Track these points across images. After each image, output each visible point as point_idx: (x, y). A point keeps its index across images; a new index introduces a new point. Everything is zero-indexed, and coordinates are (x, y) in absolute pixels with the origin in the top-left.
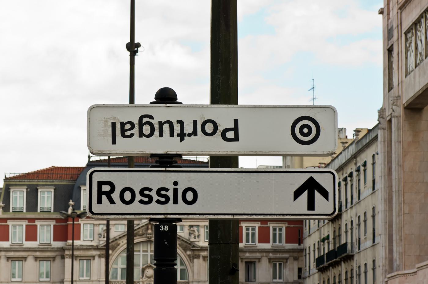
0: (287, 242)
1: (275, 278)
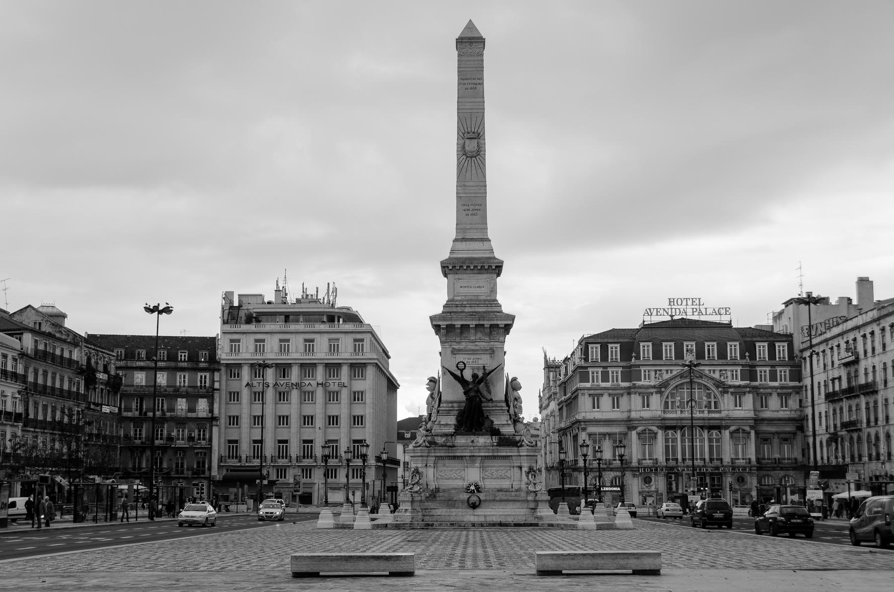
0: (790, 381)
1: (782, 407)
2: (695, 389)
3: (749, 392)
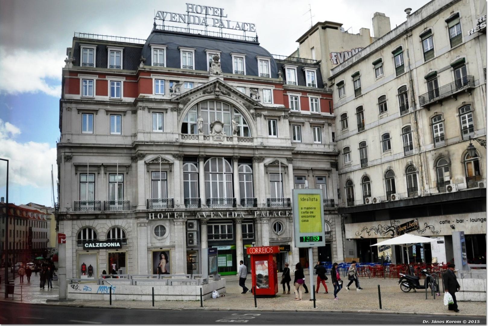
1: (315, 140)
3: (285, 117)
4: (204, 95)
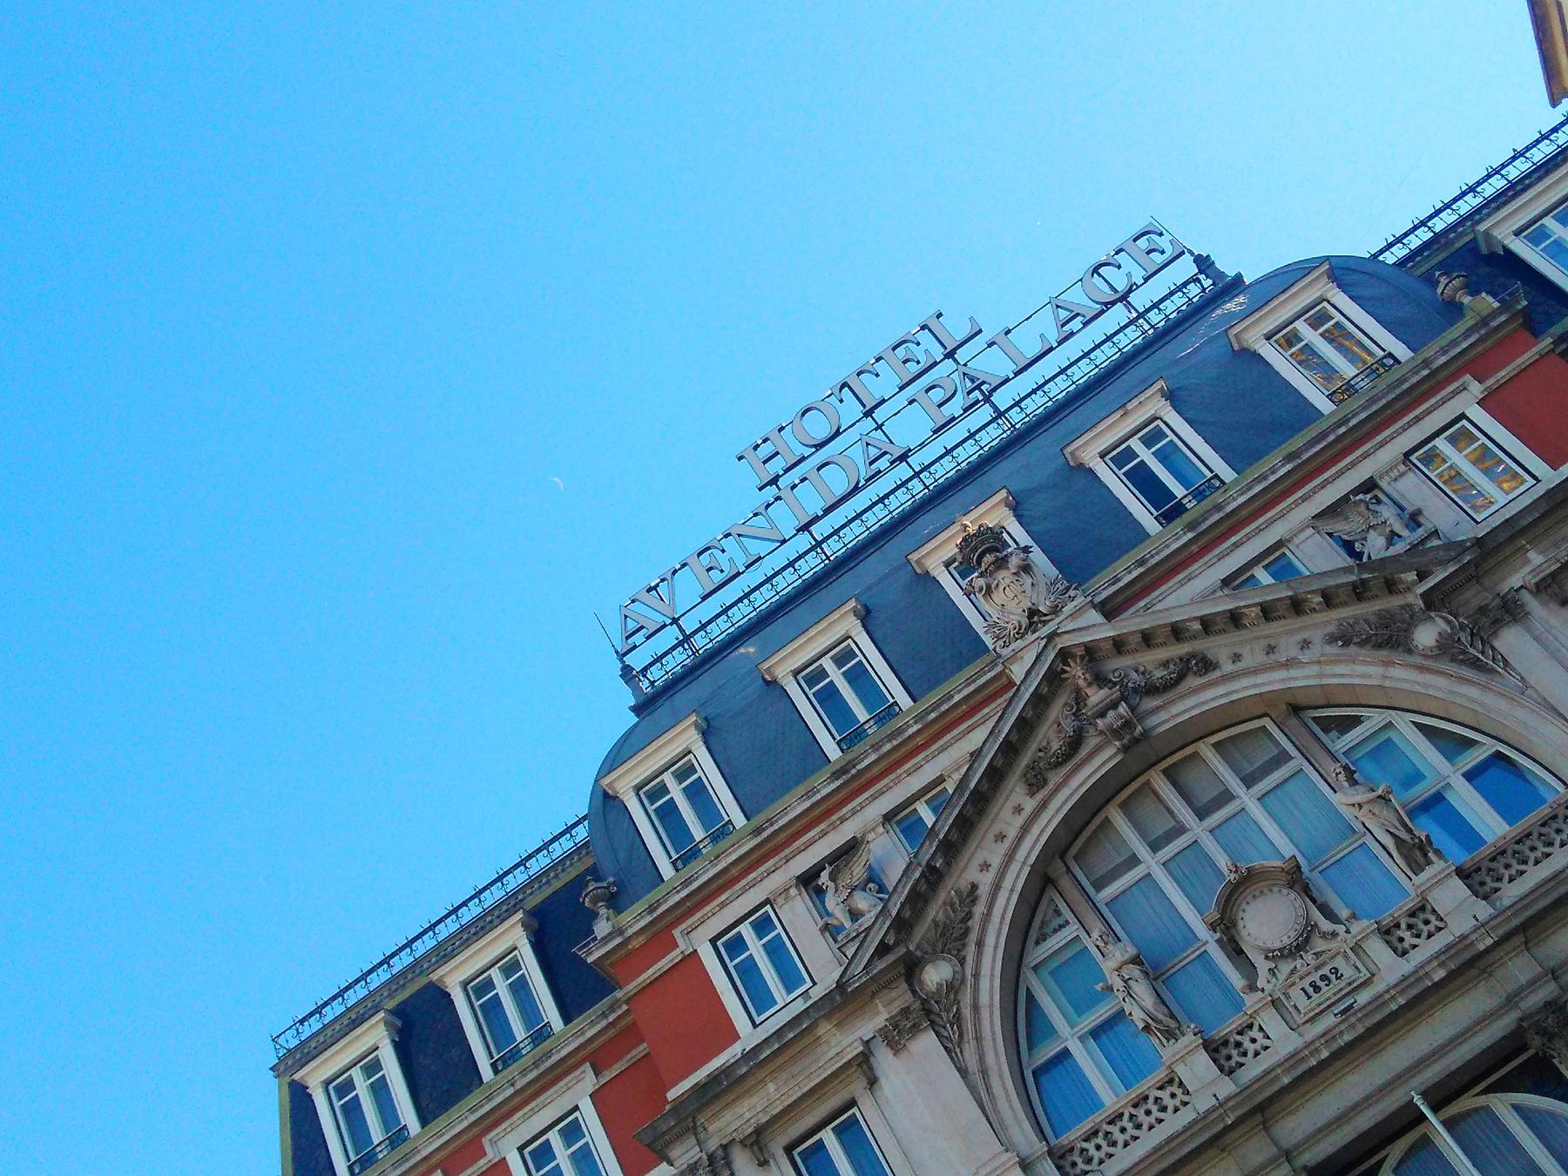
2: (1226, 797)
4: (1039, 796)
